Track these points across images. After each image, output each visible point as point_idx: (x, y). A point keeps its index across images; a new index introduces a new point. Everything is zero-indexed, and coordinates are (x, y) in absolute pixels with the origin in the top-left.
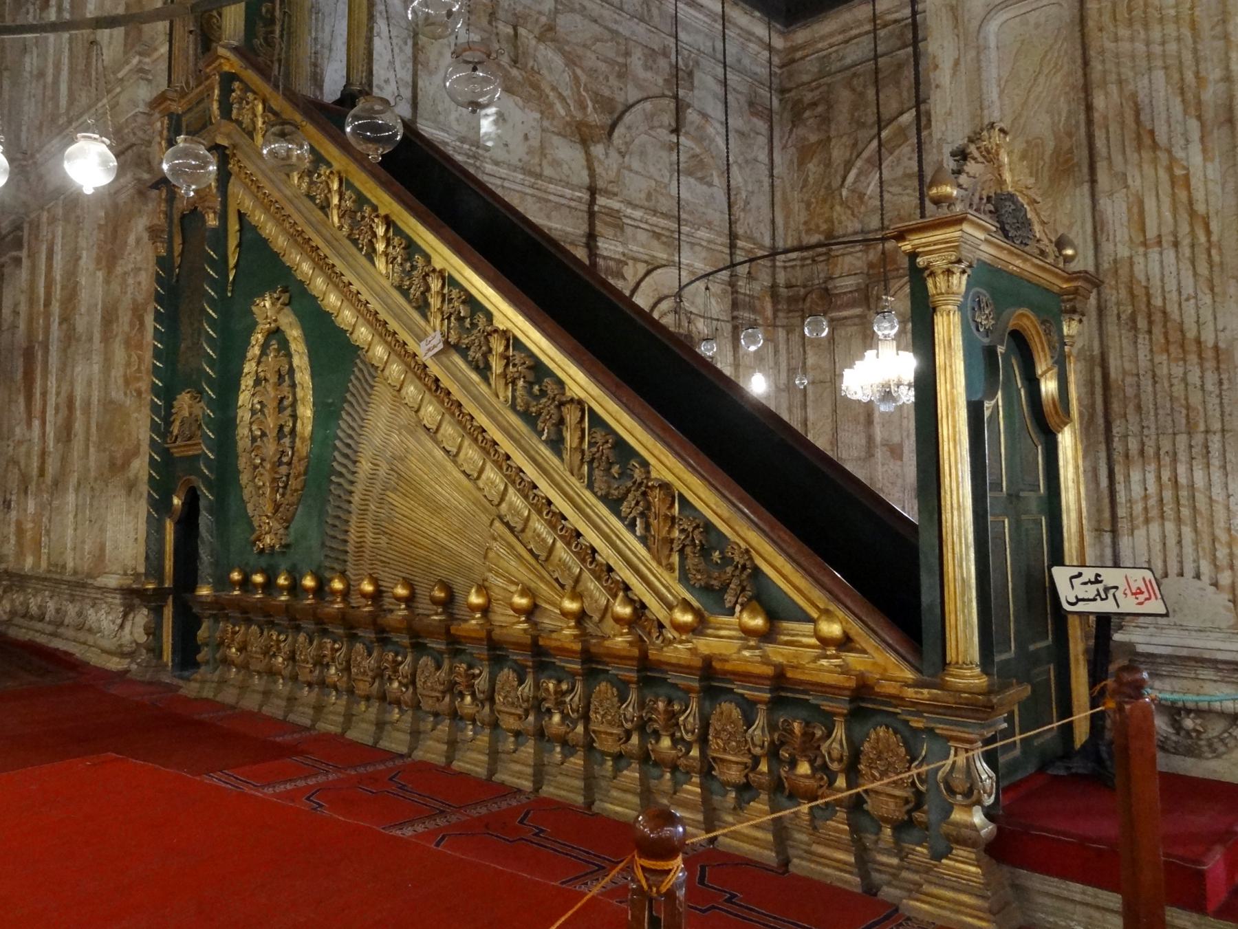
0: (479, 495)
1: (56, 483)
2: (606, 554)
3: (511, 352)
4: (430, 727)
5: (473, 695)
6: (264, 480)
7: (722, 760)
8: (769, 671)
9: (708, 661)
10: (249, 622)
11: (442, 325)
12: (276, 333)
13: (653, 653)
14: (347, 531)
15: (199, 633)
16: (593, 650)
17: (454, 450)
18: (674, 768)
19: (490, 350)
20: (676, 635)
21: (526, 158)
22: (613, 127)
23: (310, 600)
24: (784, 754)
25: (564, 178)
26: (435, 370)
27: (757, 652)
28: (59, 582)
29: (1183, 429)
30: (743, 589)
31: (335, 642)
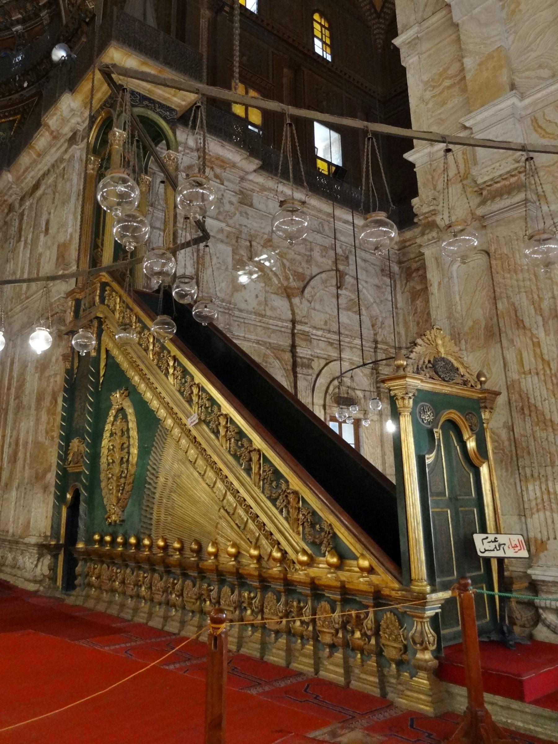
1: (6, 485)
2: (270, 527)
3: (229, 425)
4: (190, 618)
5: (210, 600)
6: (113, 486)
8: (338, 584)
10: (102, 562)
12: (121, 410)
15: (77, 568)
16: (264, 575)
17: (203, 473)
18: (302, 637)
19: (219, 424)
20: (300, 567)
21: (256, 307)
22: (305, 287)
23: (133, 550)
25: (278, 316)
26: (194, 432)
27: (334, 575)
28: (4, 540)
29: (549, 463)
30: (329, 544)
31: (144, 573)
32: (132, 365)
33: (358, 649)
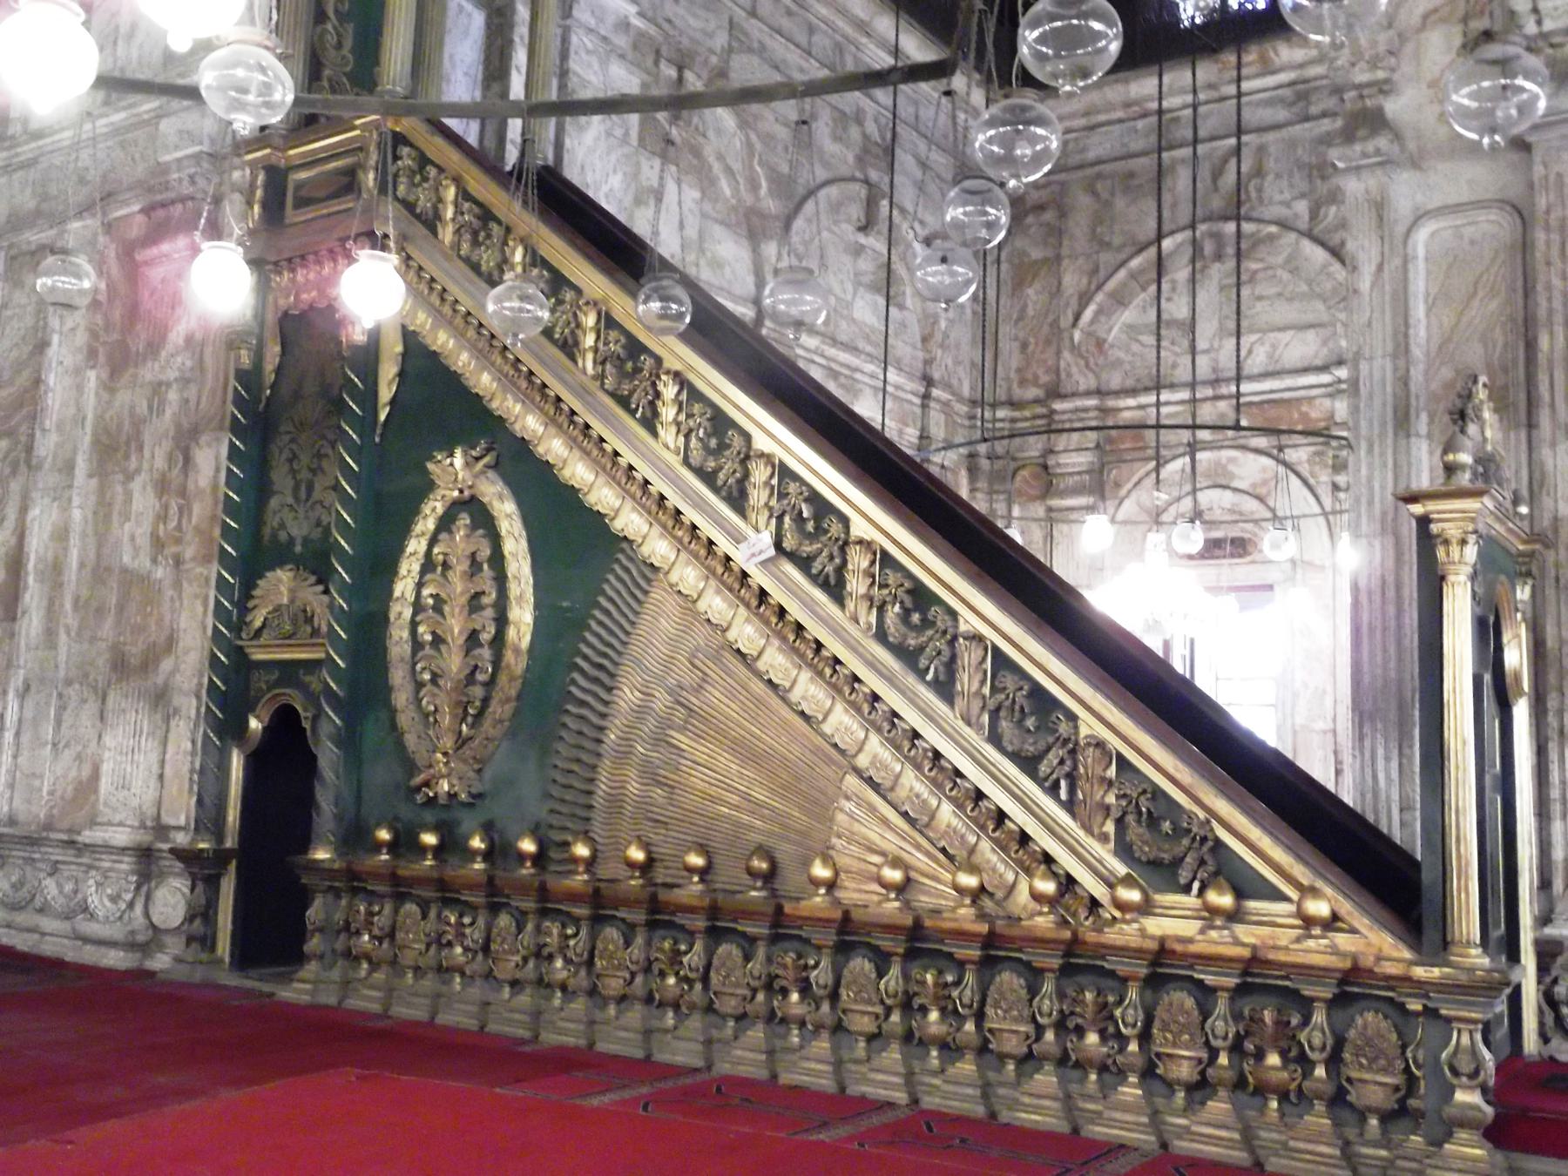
0: (819, 740)
6: (441, 702)
7: (1169, 1056)
9: (1162, 940)
11: (768, 524)
13: (1091, 937)
14: (592, 780)
15: (311, 913)
18: (1103, 1069)
20: (1117, 914)
23: (527, 870)
24: (1249, 1046)
25: (725, 285)
26: (759, 578)
32: (514, 384)
33: (1274, 1092)
